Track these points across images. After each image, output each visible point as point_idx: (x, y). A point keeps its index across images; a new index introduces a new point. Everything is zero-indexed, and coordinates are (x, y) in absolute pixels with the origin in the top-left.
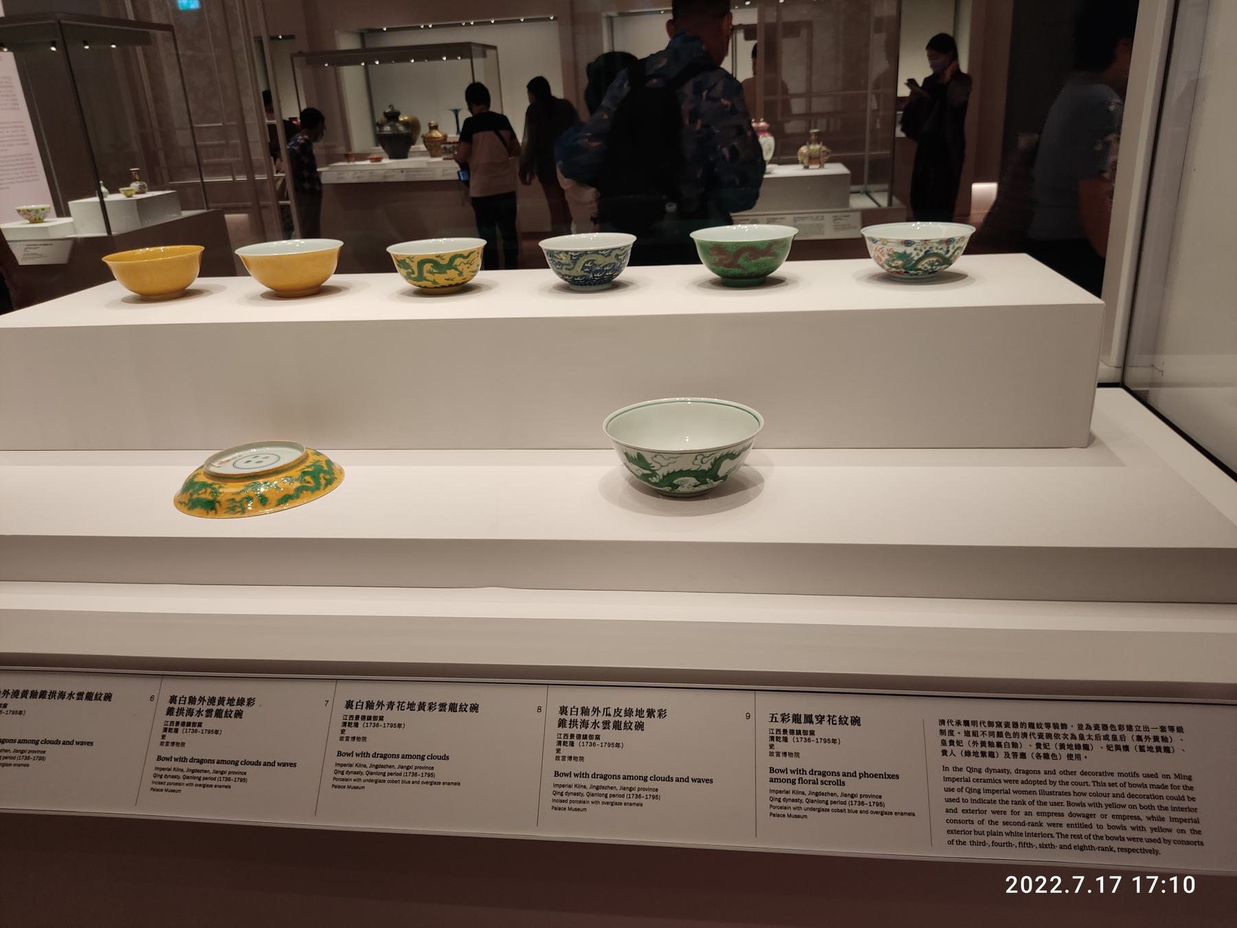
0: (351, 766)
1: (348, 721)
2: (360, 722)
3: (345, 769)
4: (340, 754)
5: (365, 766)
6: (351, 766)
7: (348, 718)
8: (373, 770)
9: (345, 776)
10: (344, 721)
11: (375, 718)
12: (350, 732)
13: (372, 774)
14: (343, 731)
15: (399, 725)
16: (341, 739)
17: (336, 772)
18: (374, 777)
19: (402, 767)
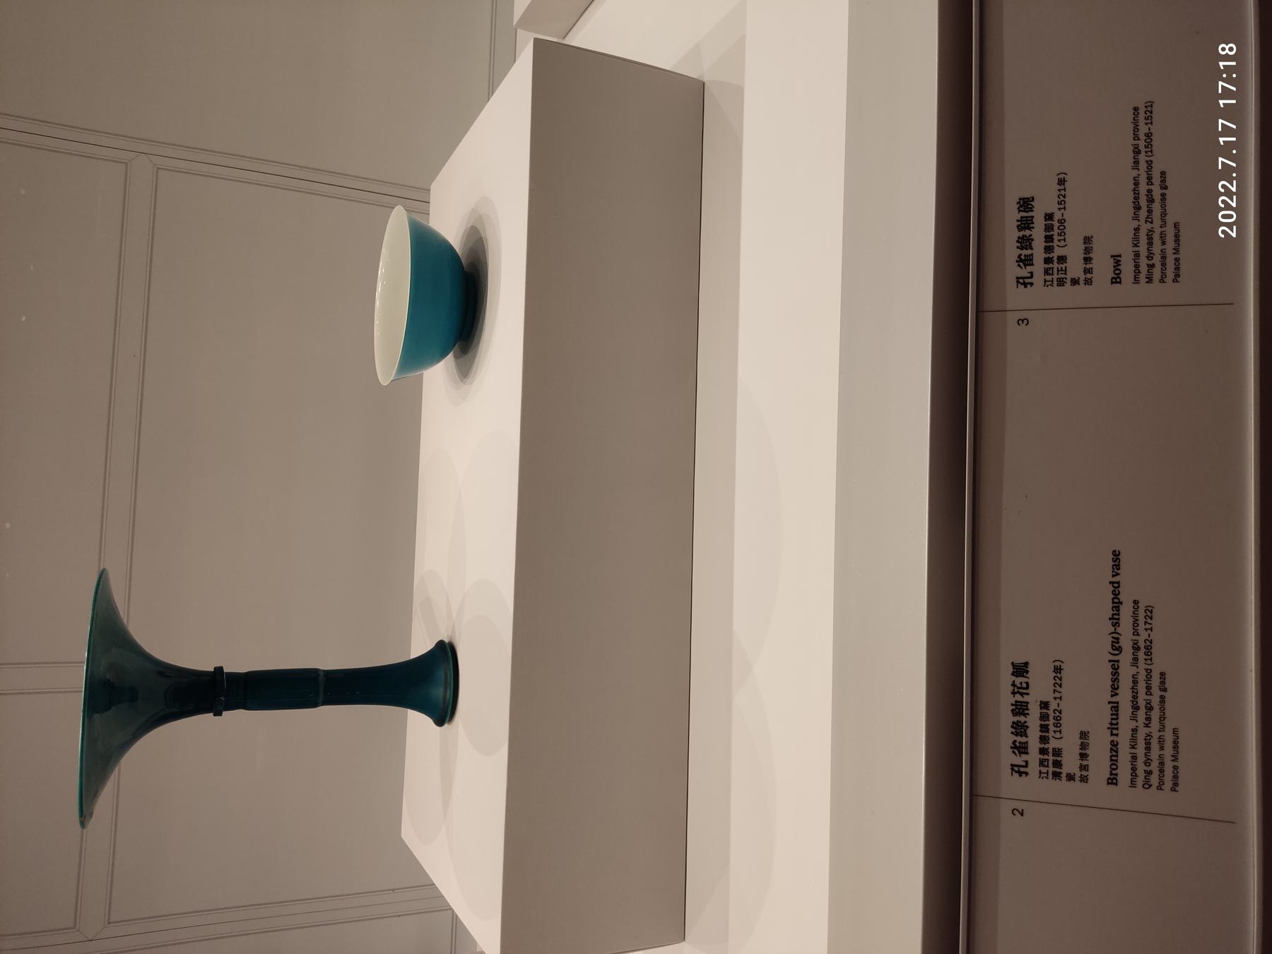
0: (1134, 758)
1: (1051, 769)
2: (1053, 744)
3: (1141, 768)
4: (1112, 781)
5: (1135, 730)
6: (1134, 758)
7: (1044, 770)
8: (1141, 714)
9: (1154, 766)
10: (1050, 776)
11: (1044, 717)
12: (1071, 763)
13: (1149, 719)
14: (1070, 777)
15: (1058, 670)
16: (1084, 779)
17: (1146, 784)
18: (1155, 714)
19: (1136, 659)
